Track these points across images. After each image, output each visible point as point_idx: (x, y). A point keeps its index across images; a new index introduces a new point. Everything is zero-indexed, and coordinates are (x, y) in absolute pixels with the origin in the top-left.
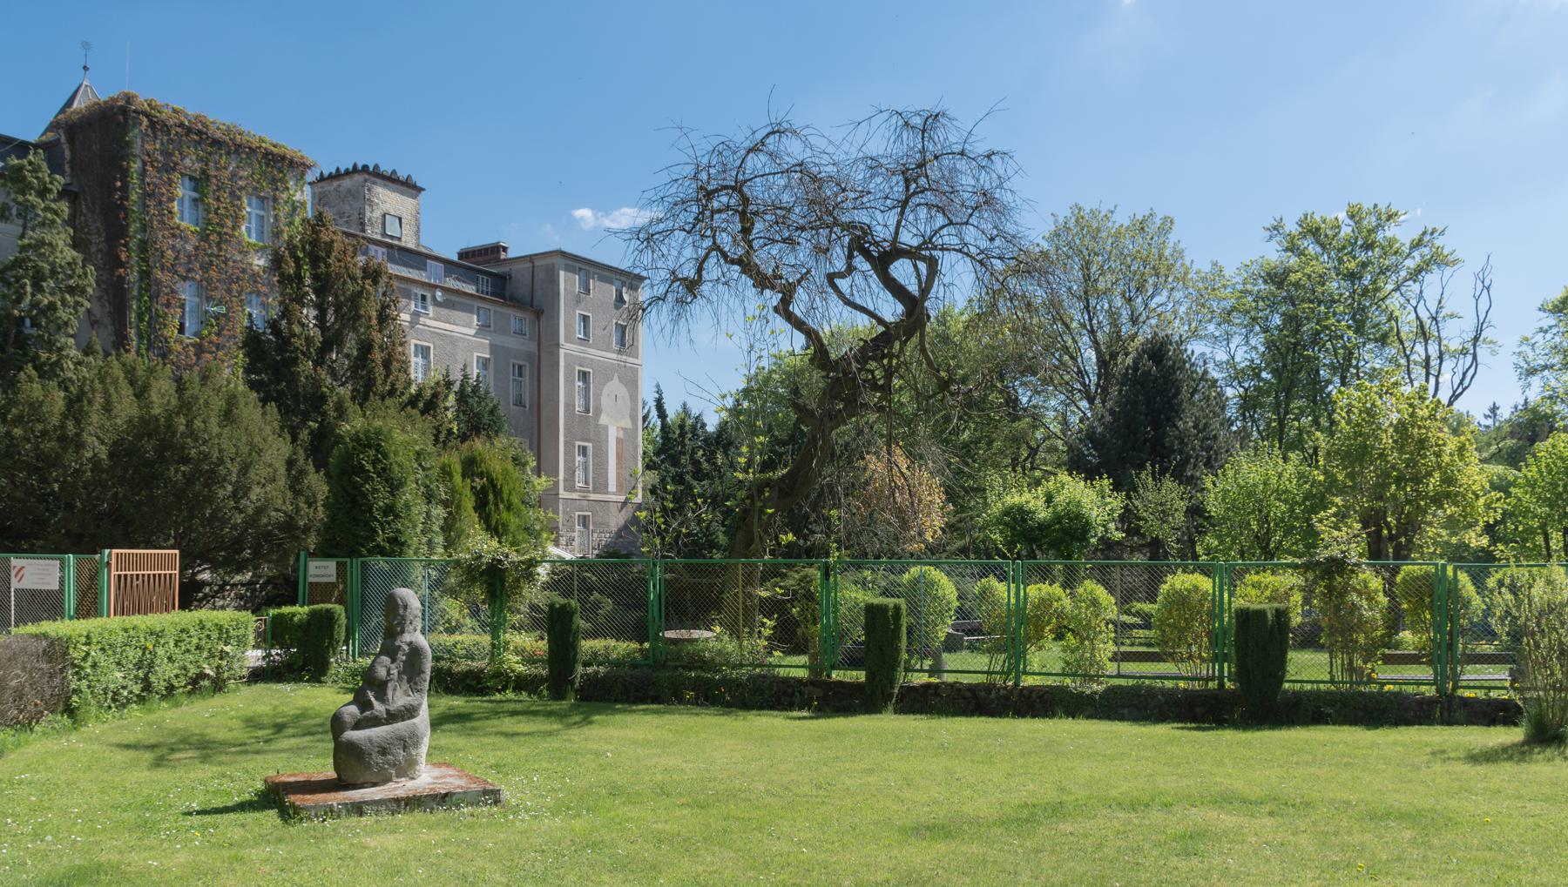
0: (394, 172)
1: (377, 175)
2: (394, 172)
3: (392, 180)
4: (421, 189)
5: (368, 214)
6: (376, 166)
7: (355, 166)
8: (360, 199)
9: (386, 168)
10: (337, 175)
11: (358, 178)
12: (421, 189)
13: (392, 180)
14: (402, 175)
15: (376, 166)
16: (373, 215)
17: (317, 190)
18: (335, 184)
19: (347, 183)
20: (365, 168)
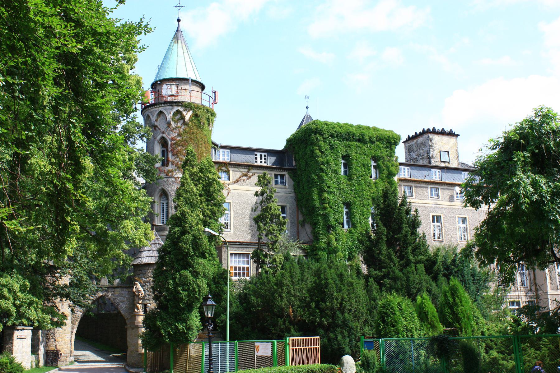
0: (443, 129)
1: (435, 132)
2: (443, 129)
3: (443, 133)
4: (458, 135)
5: (431, 153)
6: (434, 129)
7: (424, 130)
8: (427, 145)
9: (439, 128)
10: (416, 136)
11: (425, 136)
12: (458, 135)
13: (443, 133)
14: (447, 130)
15: (434, 129)
16: (434, 153)
17: (407, 145)
18: (415, 141)
19: (420, 140)
20: (429, 130)
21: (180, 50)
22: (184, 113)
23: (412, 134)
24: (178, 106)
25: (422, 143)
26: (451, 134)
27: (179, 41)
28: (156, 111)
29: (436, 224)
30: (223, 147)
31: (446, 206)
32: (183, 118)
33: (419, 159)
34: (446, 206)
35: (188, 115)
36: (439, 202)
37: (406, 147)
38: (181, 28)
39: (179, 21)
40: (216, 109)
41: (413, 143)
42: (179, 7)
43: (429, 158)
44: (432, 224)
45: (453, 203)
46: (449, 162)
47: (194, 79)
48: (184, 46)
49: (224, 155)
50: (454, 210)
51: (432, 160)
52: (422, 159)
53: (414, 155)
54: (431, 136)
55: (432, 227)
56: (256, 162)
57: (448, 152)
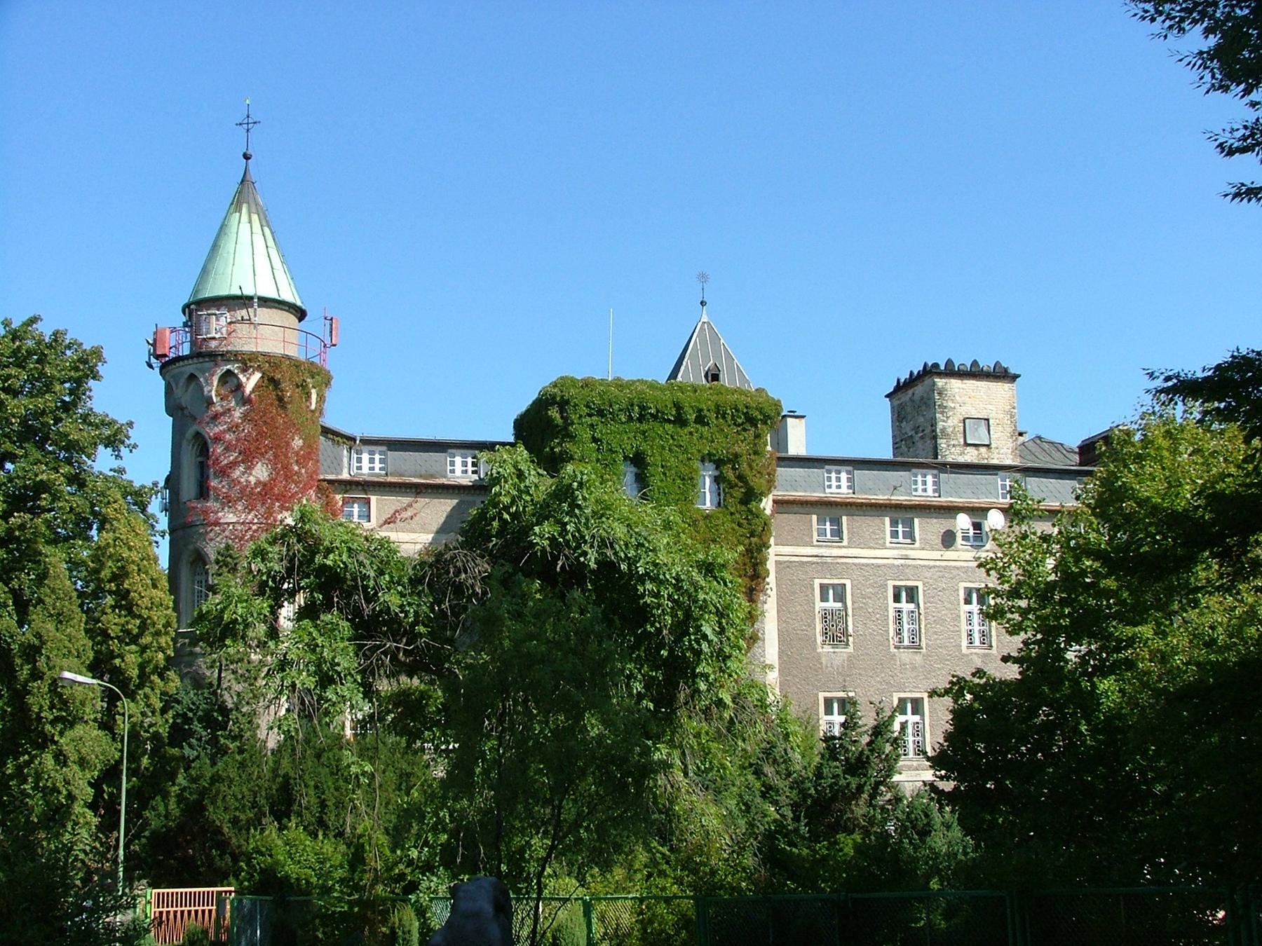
0: (975, 363)
2: (975, 363)
3: (975, 373)
4: (1014, 378)
5: (940, 425)
6: (949, 363)
9: (962, 360)
10: (913, 381)
11: (927, 381)
14: (987, 363)
15: (949, 363)
16: (949, 423)
17: (896, 403)
18: (910, 392)
19: (919, 390)
20: (936, 365)
21: (245, 226)
22: (242, 378)
23: (904, 376)
24: (229, 361)
25: (922, 398)
26: (1001, 375)
27: (244, 210)
28: (182, 373)
29: (906, 606)
30: (366, 442)
31: (932, 563)
32: (239, 386)
33: (917, 438)
34: (932, 563)
35: (251, 382)
36: (912, 554)
37: (892, 408)
38: (253, 175)
39: (247, 157)
40: (332, 363)
41: (905, 397)
42: (248, 123)
43: (935, 438)
44: (892, 605)
45: (949, 554)
46: (988, 446)
47: (272, 294)
48: (255, 217)
49: (372, 461)
50: (955, 572)
51: (942, 443)
52: (922, 438)
53: (907, 428)
54: (940, 382)
55: (892, 614)
56: (453, 471)
57: (988, 420)
